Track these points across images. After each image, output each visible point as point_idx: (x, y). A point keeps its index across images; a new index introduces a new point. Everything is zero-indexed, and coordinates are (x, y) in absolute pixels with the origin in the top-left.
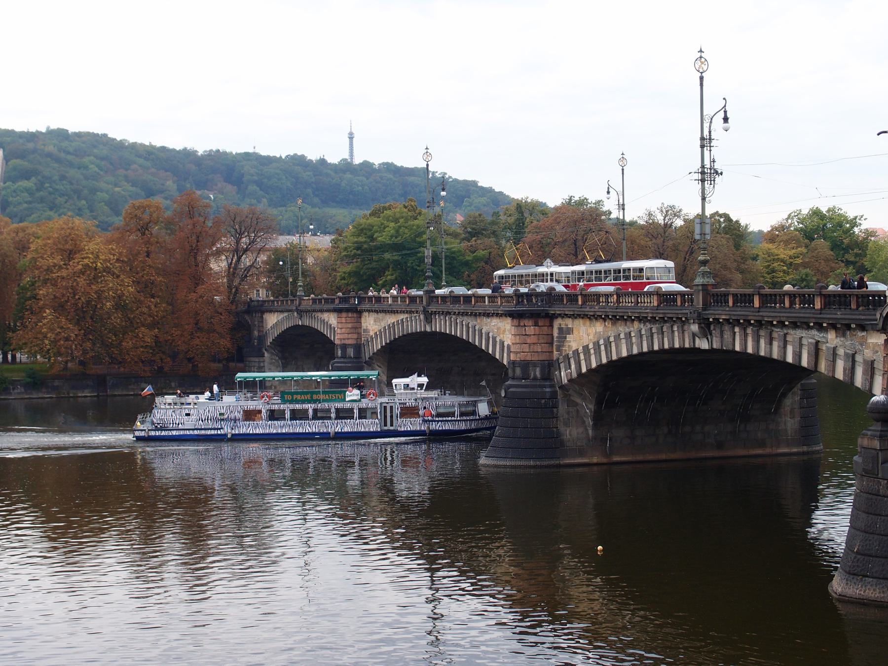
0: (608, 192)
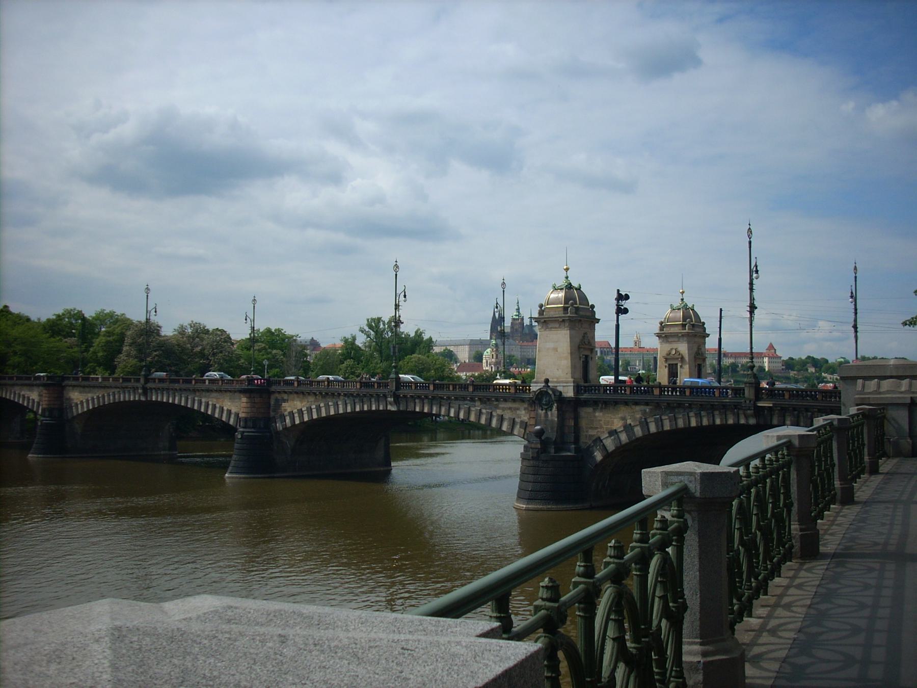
0: (246, 319)
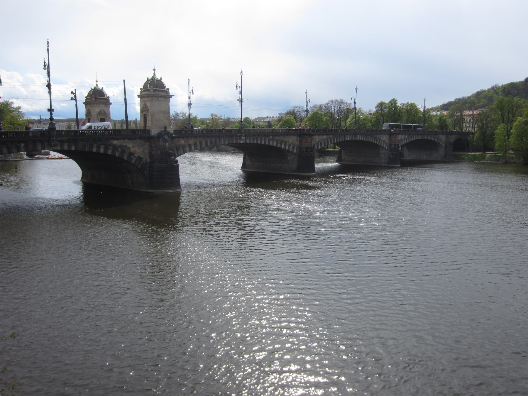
0: (352, 99)
